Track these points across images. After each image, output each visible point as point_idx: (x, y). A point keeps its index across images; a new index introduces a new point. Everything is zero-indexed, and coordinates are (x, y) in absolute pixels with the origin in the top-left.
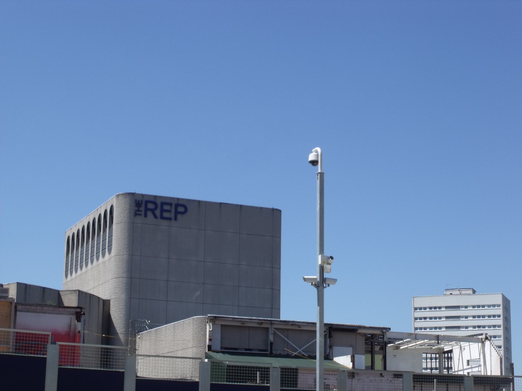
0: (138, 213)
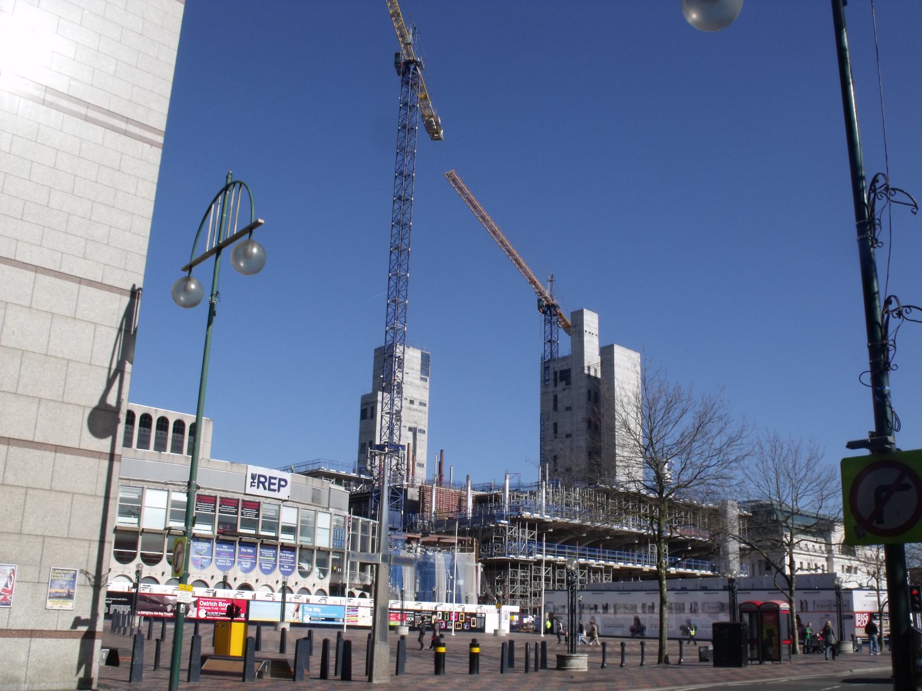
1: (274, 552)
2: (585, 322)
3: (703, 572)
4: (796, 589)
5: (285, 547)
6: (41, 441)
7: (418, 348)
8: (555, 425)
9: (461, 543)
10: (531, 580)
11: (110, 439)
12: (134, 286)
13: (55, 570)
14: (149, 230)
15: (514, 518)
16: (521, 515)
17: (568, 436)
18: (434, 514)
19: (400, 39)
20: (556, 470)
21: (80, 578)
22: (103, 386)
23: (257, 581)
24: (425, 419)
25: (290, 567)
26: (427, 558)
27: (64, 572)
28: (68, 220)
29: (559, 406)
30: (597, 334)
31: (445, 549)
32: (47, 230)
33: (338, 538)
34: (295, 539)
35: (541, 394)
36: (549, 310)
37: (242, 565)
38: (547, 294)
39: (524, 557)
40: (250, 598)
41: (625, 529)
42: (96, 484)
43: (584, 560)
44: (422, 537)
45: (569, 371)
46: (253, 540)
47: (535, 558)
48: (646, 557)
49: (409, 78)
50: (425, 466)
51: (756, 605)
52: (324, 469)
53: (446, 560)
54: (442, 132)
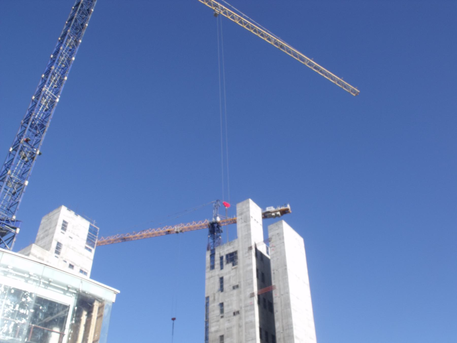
8: (222, 305)
29: (225, 286)
45: (236, 252)
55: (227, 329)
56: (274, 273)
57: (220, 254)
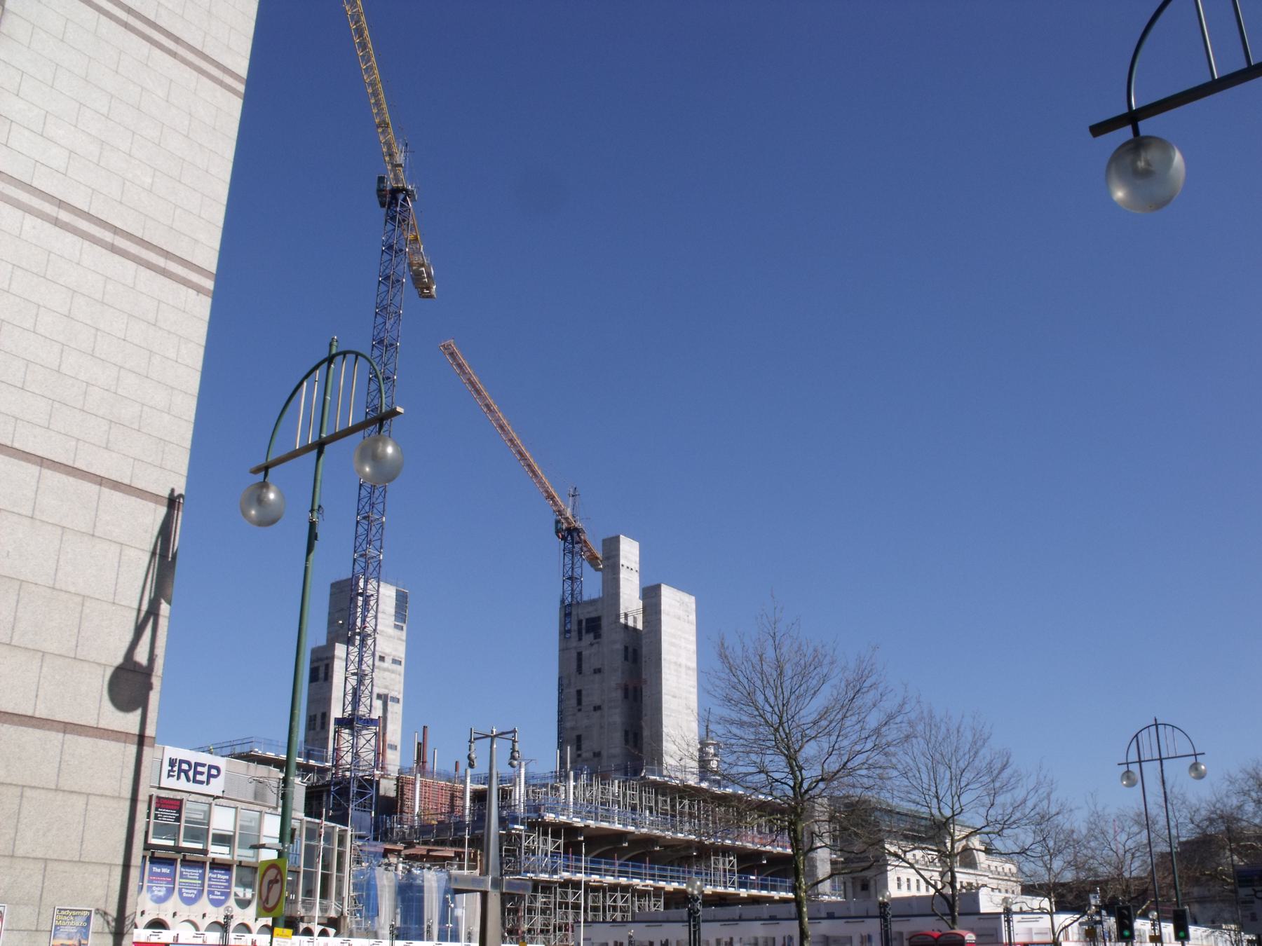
0: (171, 773)
1: (201, 871)
2: (622, 553)
3: (783, 894)
4: (959, 914)
5: (217, 865)
6: (44, 716)
7: (391, 584)
8: (579, 693)
9: (460, 856)
10: (555, 909)
11: (139, 712)
12: (173, 490)
13: (60, 910)
14: (194, 412)
15: (532, 822)
16: (543, 818)
17: (597, 708)
18: (418, 816)
19: (387, 159)
20: (579, 756)
21: (96, 922)
22: (129, 637)
23: (175, 914)
24: (400, 682)
25: (222, 894)
26: (412, 879)
27: (74, 913)
28: (86, 393)
29: (585, 666)
30: (638, 570)
31: (436, 865)
32: (57, 405)
33: (295, 852)
34: (231, 852)
35: (560, 651)
36: (570, 535)
37: (153, 891)
38: (569, 513)
39: (547, 876)
40: (171, 941)
41: (680, 836)
42: (121, 780)
43: (625, 879)
44: (405, 848)
45: (598, 619)
46: (171, 854)
47: (561, 878)
48: (707, 874)
49: (396, 212)
50: (399, 748)
51: (933, 937)
52: (259, 751)
53: (438, 881)
54: (434, 287)
55: (586, 727)
56: (645, 662)
57: (578, 615)
